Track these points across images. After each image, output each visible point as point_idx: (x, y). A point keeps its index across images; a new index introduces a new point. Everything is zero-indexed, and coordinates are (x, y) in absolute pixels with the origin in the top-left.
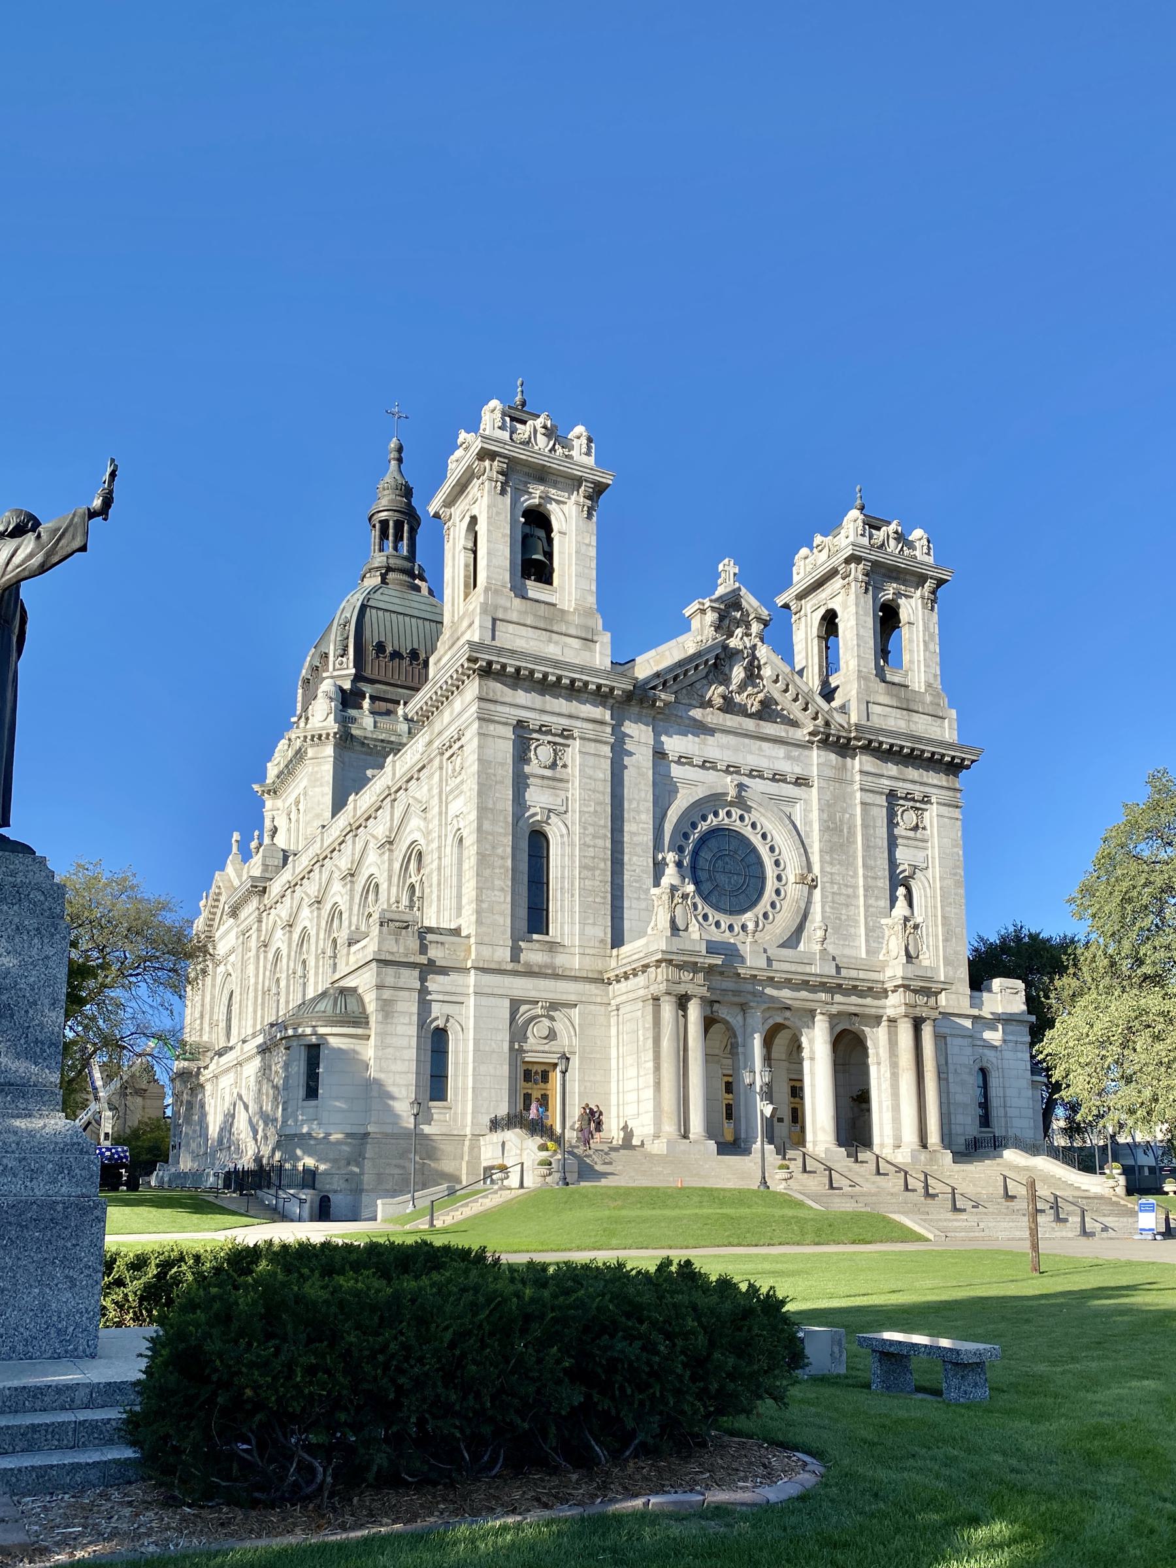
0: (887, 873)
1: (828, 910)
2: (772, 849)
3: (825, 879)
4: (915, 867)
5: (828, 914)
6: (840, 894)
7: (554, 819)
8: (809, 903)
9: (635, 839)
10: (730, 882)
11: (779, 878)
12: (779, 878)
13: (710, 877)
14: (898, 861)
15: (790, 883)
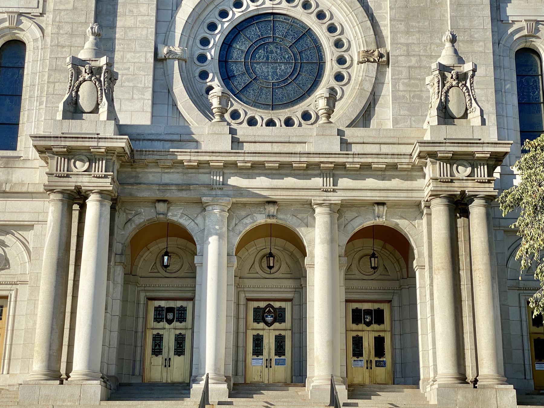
0: (489, 34)
1: (401, 88)
2: (332, 29)
3: (398, 52)
4: (538, 22)
5: (401, 94)
6: (420, 67)
7: (26, 23)
8: (378, 83)
9: (130, 34)
10: (275, 73)
11: (341, 61)
12: (341, 61)
13: (247, 70)
14: (510, 19)
15: (355, 62)
